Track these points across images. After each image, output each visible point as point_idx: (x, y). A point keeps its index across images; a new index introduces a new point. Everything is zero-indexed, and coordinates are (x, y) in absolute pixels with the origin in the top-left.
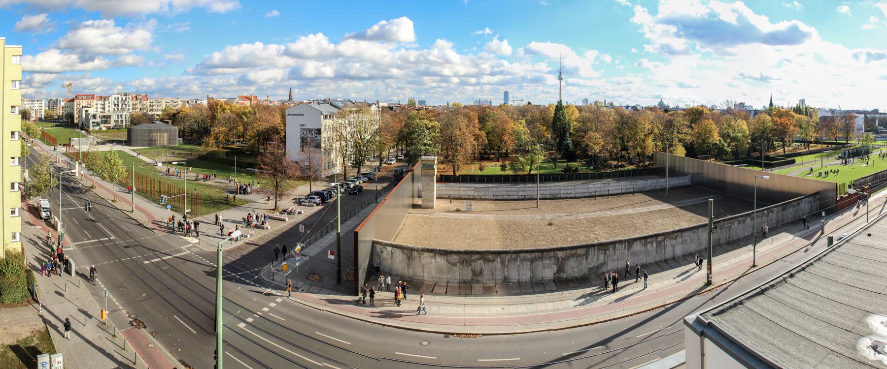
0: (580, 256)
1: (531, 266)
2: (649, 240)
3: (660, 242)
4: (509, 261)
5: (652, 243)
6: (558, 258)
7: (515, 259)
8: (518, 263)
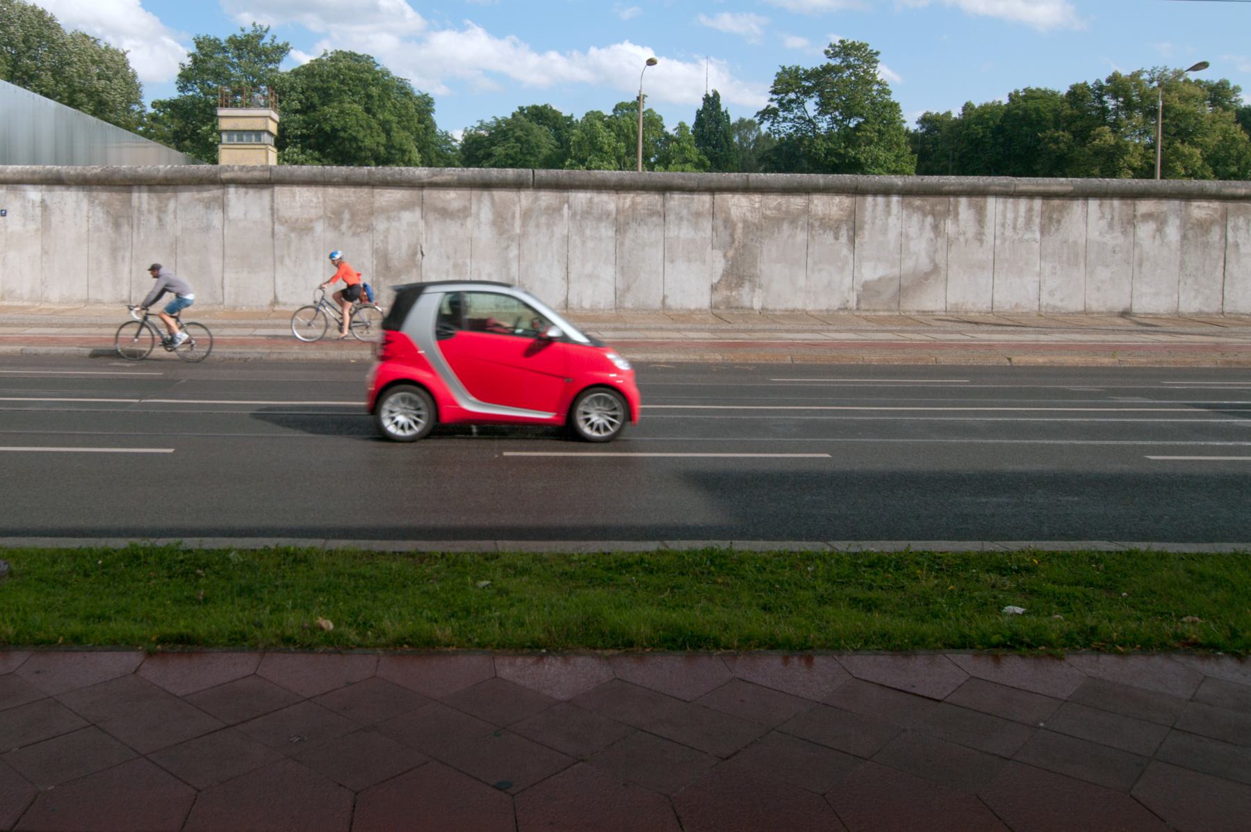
0: (827, 224)
1: (619, 245)
2: (1145, 206)
3: (1203, 227)
4: (526, 215)
5: (1161, 221)
6: (728, 223)
7: (554, 211)
8: (561, 229)
